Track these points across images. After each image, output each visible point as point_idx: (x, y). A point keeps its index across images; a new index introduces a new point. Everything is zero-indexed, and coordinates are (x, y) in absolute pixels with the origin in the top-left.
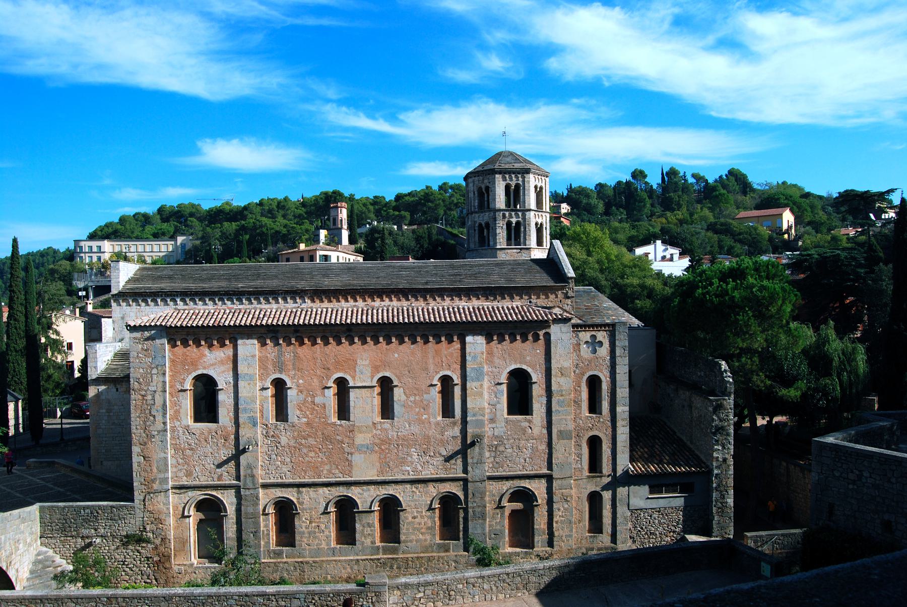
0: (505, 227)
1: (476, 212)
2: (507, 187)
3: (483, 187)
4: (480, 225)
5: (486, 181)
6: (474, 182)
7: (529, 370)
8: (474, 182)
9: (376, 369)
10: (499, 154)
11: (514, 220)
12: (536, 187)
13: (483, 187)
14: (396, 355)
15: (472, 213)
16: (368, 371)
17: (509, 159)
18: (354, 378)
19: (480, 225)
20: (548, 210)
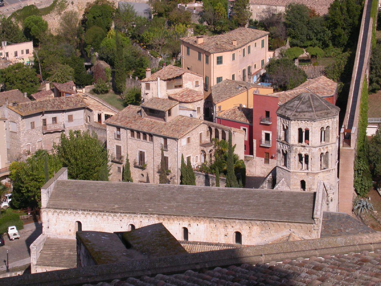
11: (303, 154)
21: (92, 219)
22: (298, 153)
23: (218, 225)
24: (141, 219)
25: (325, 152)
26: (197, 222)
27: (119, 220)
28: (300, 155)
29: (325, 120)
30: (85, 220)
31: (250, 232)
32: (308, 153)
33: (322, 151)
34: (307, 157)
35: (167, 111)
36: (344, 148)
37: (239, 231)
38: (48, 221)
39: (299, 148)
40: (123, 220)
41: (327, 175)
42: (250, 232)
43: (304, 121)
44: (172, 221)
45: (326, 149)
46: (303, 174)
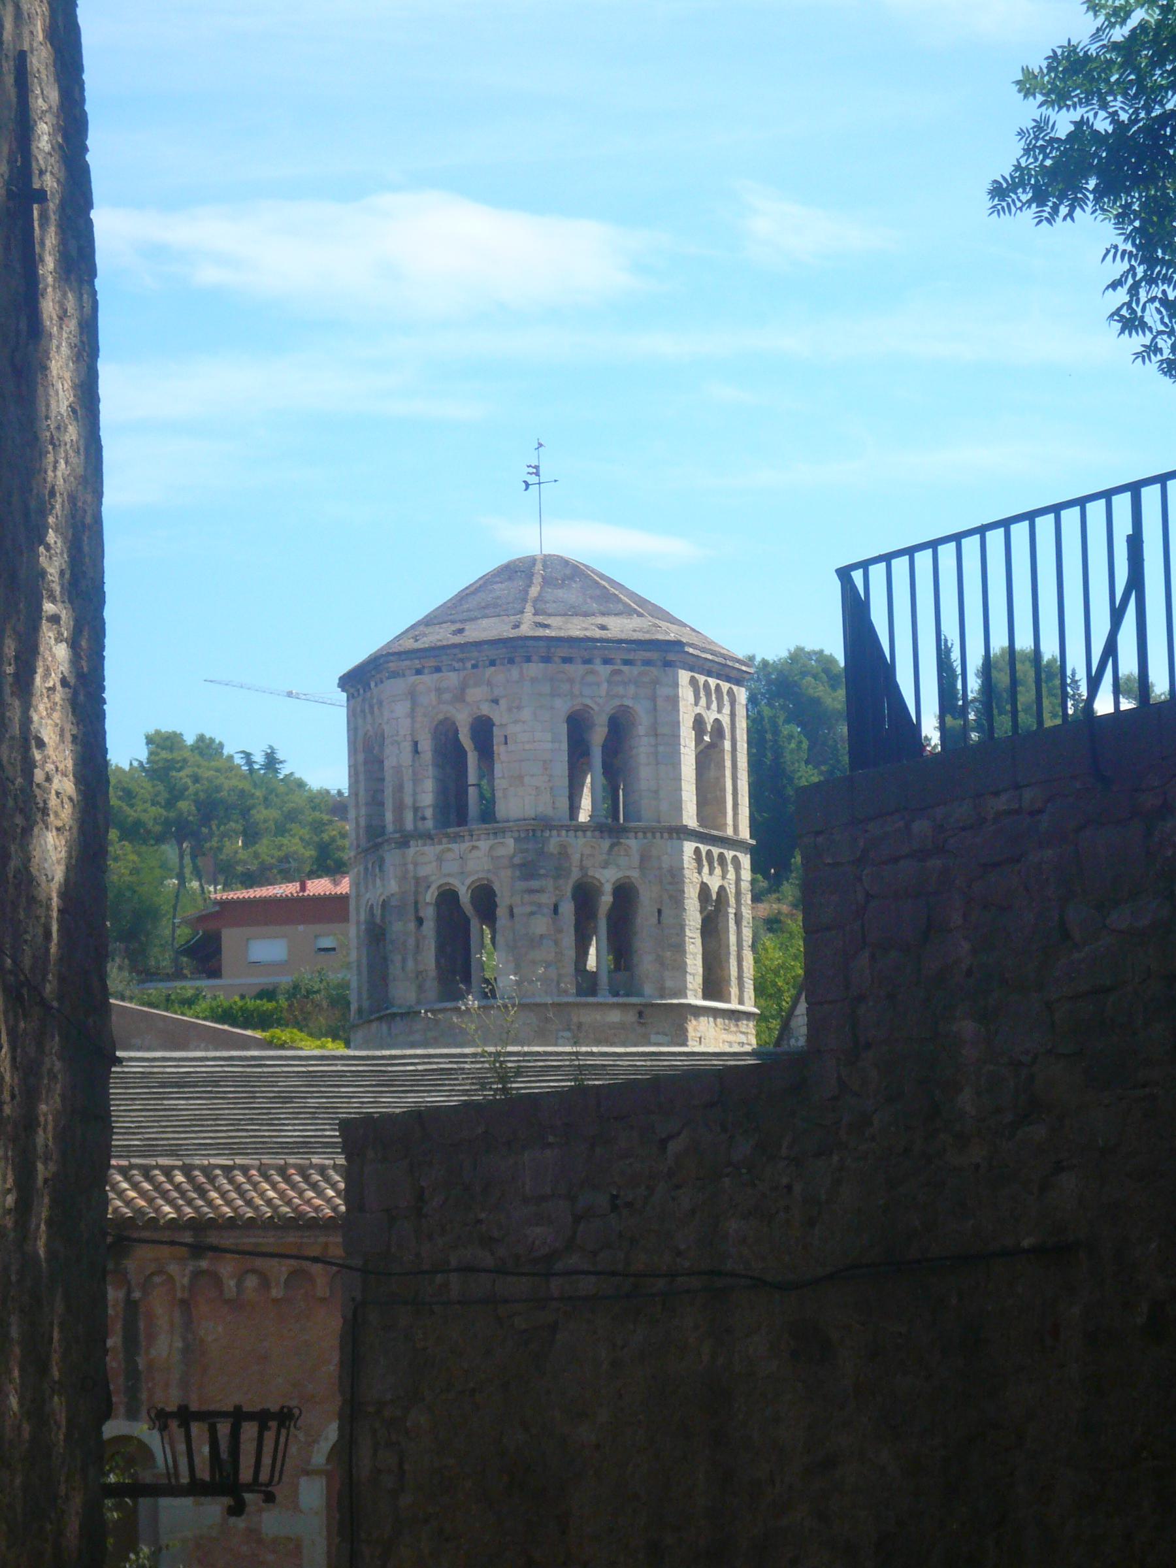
0: (568, 909)
1: (427, 837)
2: (577, 726)
3: (463, 719)
4: (448, 897)
5: (476, 694)
6: (412, 695)
8: (412, 695)
10: (517, 572)
11: (607, 878)
12: (699, 722)
13: (463, 719)
15: (404, 842)
17: (571, 595)
19: (448, 897)
20: (745, 833)
22: (575, 874)
32: (635, 874)
43: (607, 661)
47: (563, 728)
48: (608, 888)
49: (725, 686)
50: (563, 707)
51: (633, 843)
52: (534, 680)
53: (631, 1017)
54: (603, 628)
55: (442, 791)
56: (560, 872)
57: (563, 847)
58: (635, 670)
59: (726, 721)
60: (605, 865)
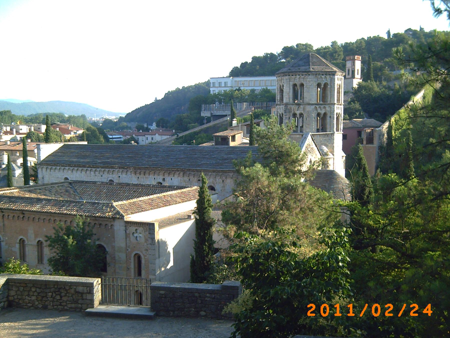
7: (105, 246)
9: (36, 236)
11: (298, 113)
14: (45, 230)
16: (33, 236)
18: (27, 239)
21: (78, 175)
22: (293, 112)
23: (191, 177)
24: (120, 174)
25: (322, 112)
26: (171, 176)
27: (100, 175)
28: (294, 115)
29: (323, 75)
30: (71, 176)
31: (224, 187)
32: (302, 112)
33: (319, 111)
34: (301, 115)
35: (230, 137)
36: (367, 145)
37: (212, 185)
38: (43, 178)
39: (293, 107)
40: (104, 176)
41: (325, 140)
42: (224, 187)
44: (147, 175)
45: (324, 110)
46: (298, 136)
47: (291, 87)
48: (298, 114)
49: (328, 77)
50: (291, 83)
51: (302, 106)
52: (286, 79)
53: (301, 136)
54: (299, 69)
55: (280, 98)
56: (290, 112)
57: (291, 108)
58: (303, 76)
59: (329, 83)
60: (298, 110)
